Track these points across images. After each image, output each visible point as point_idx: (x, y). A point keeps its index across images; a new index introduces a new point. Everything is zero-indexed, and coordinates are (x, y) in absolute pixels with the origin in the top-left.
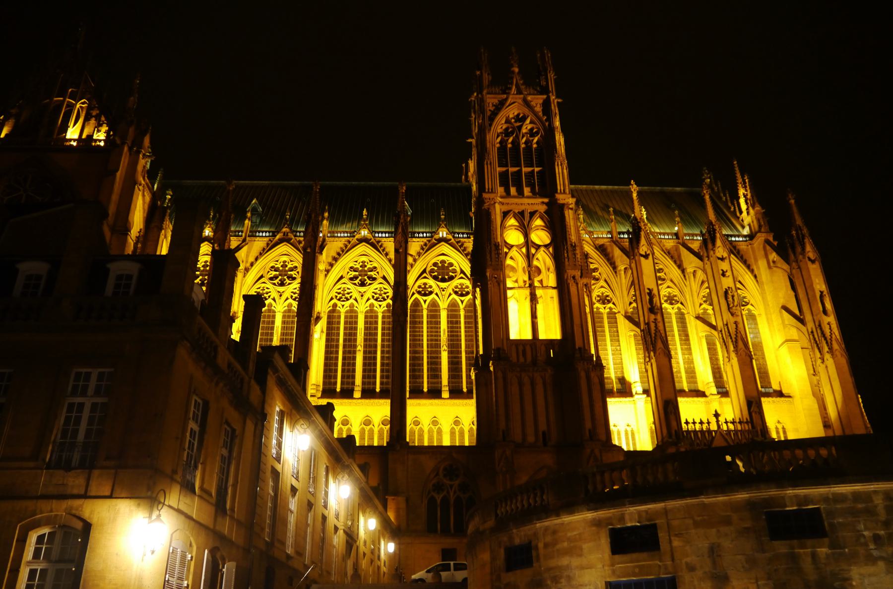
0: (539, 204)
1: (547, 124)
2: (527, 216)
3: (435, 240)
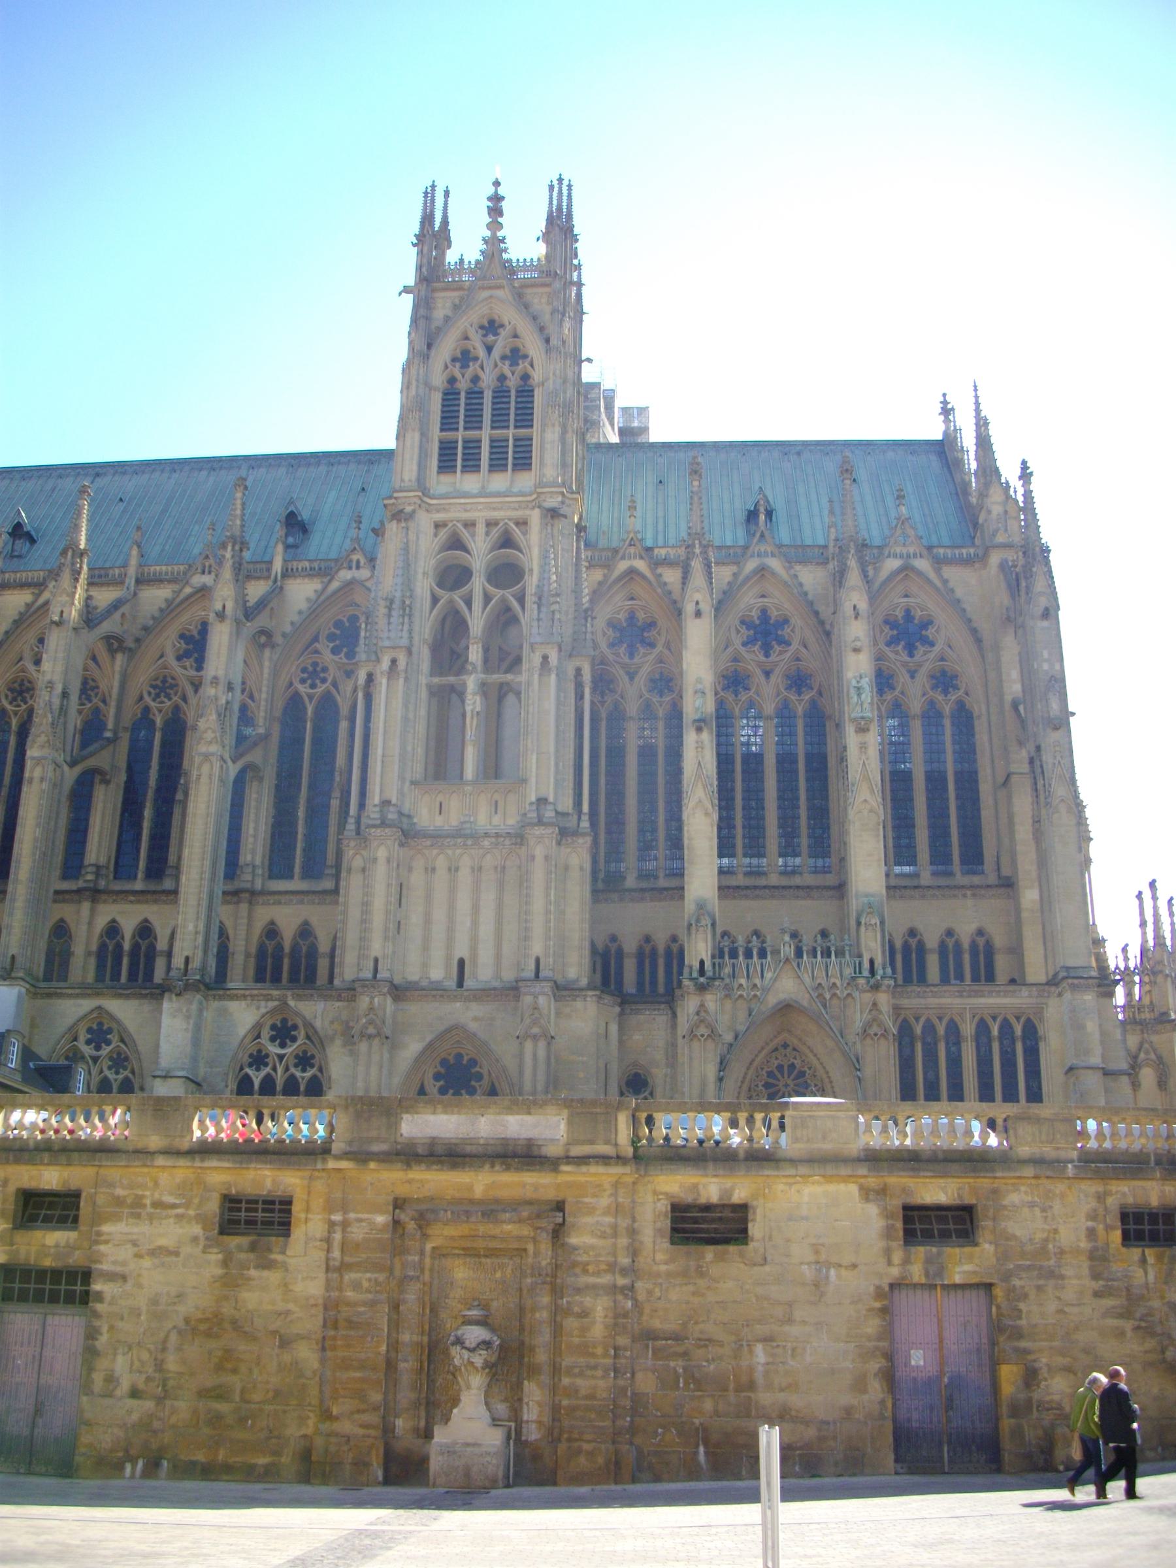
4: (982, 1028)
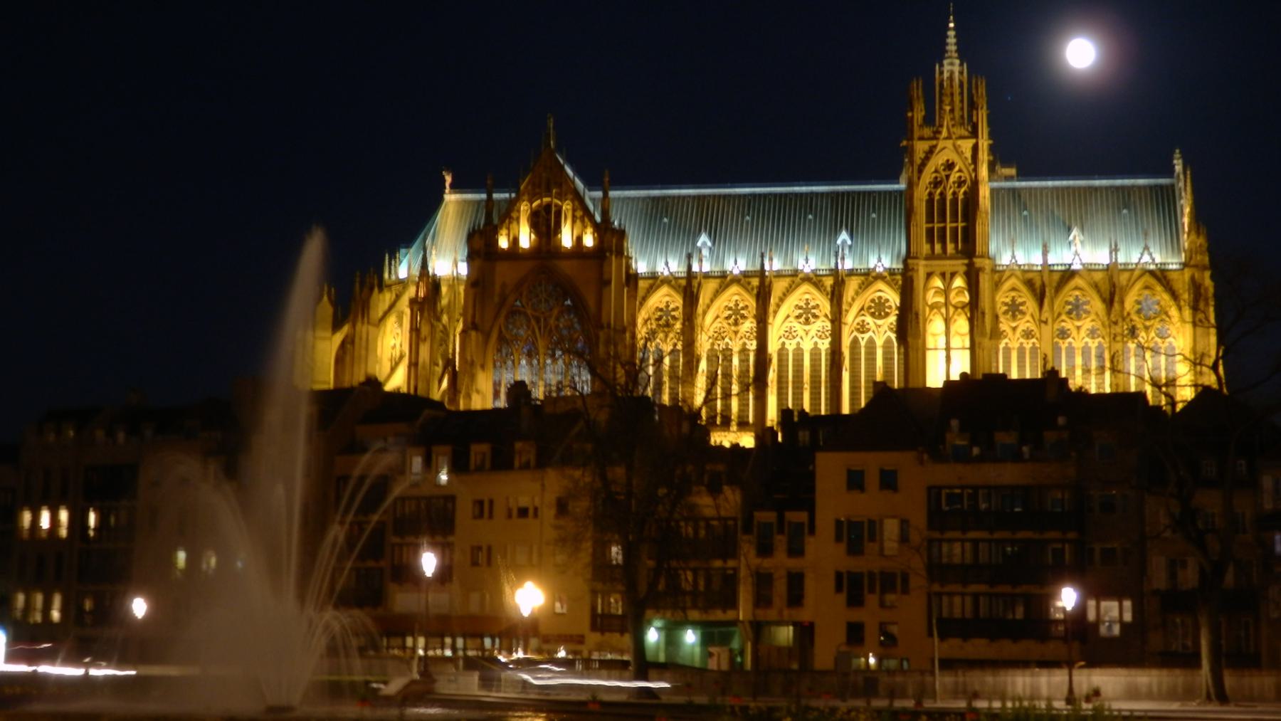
0: (960, 265)
1: (973, 175)
2: (948, 276)
3: (873, 277)
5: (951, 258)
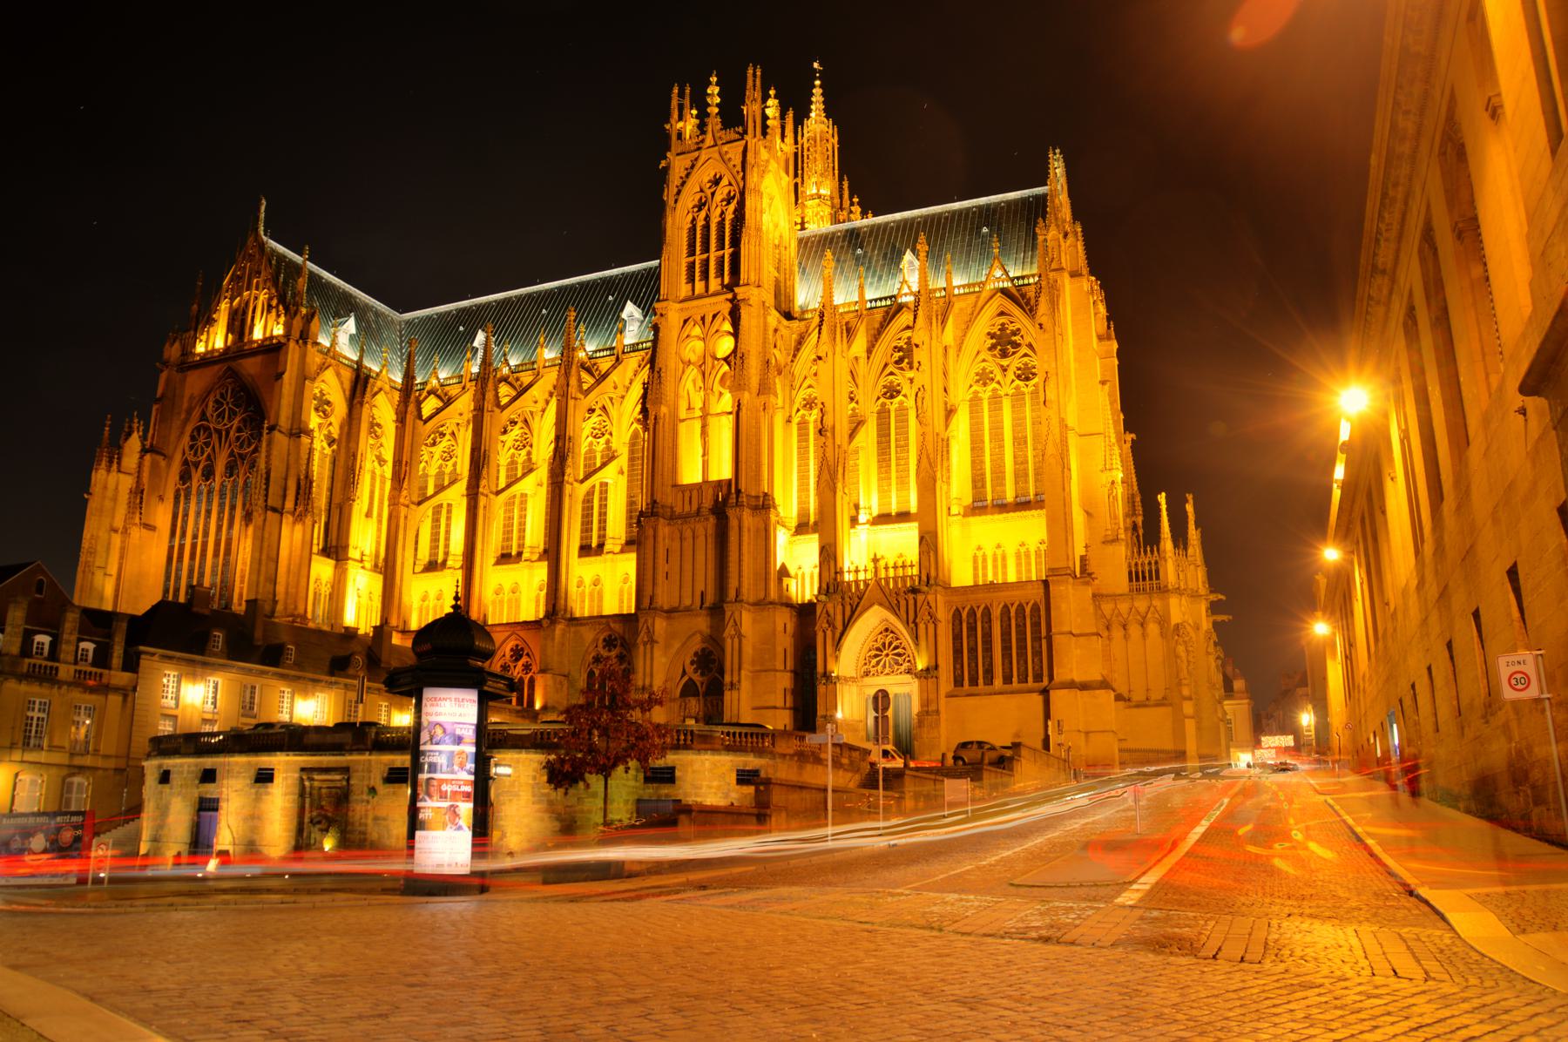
4: (1006, 609)
5: (716, 294)
